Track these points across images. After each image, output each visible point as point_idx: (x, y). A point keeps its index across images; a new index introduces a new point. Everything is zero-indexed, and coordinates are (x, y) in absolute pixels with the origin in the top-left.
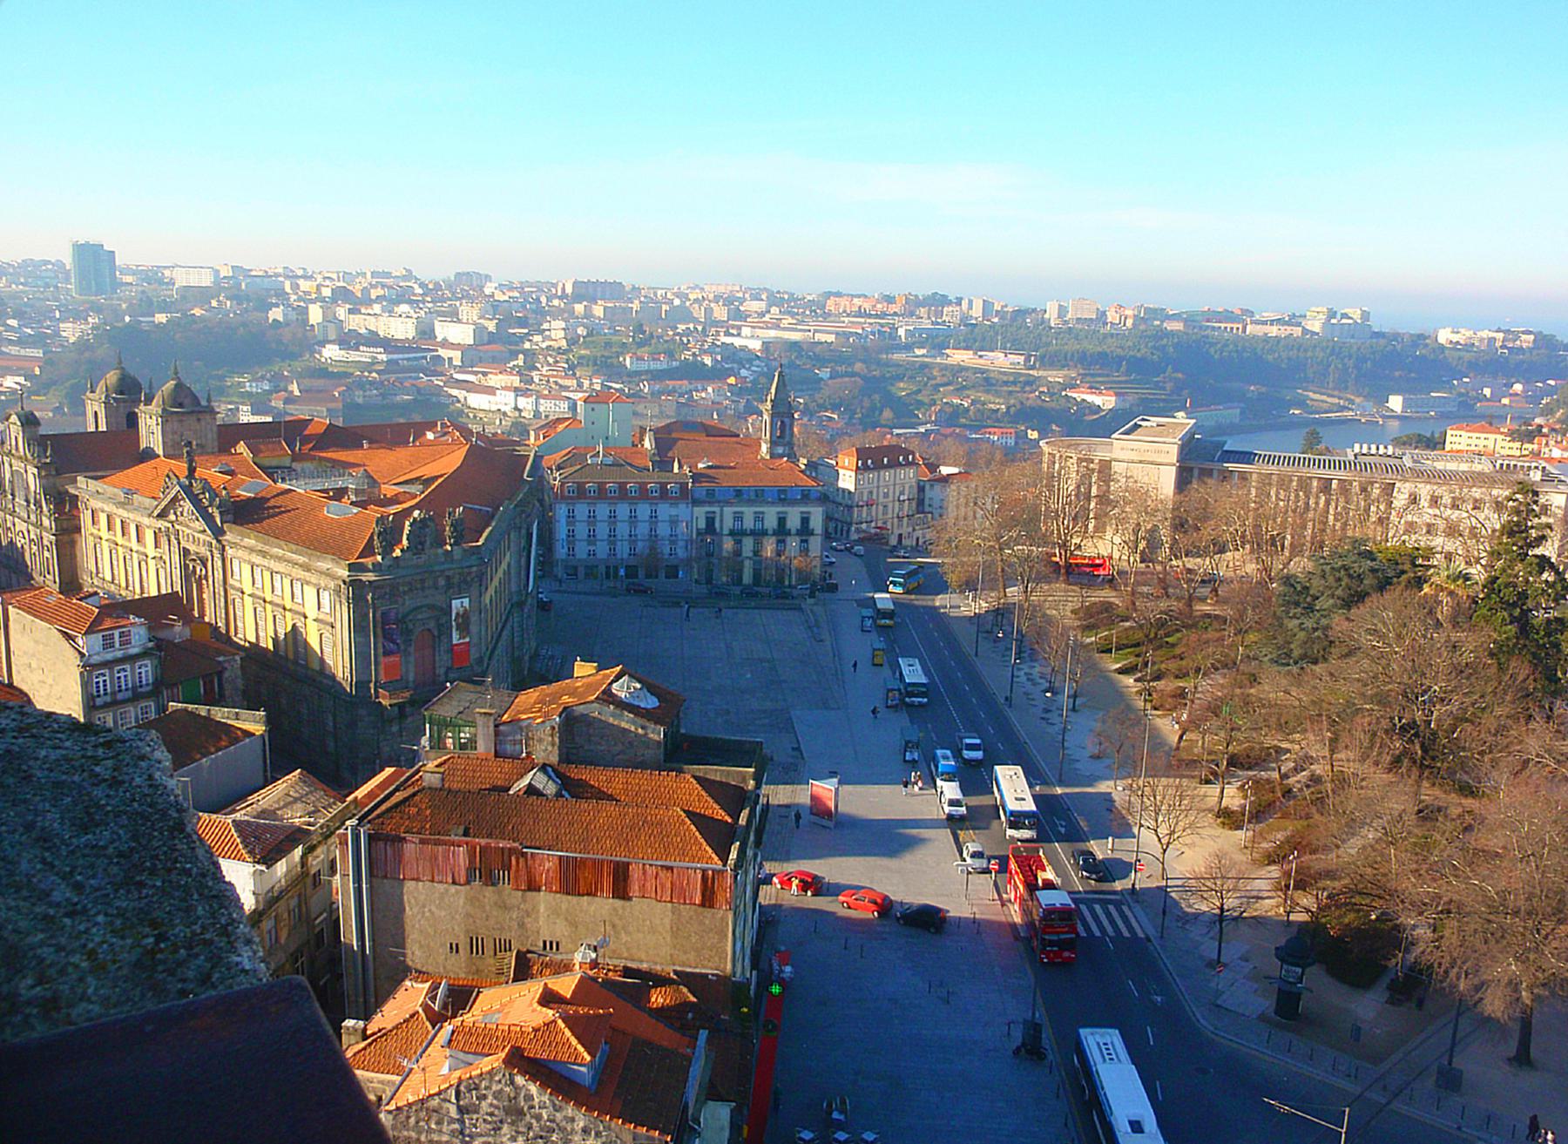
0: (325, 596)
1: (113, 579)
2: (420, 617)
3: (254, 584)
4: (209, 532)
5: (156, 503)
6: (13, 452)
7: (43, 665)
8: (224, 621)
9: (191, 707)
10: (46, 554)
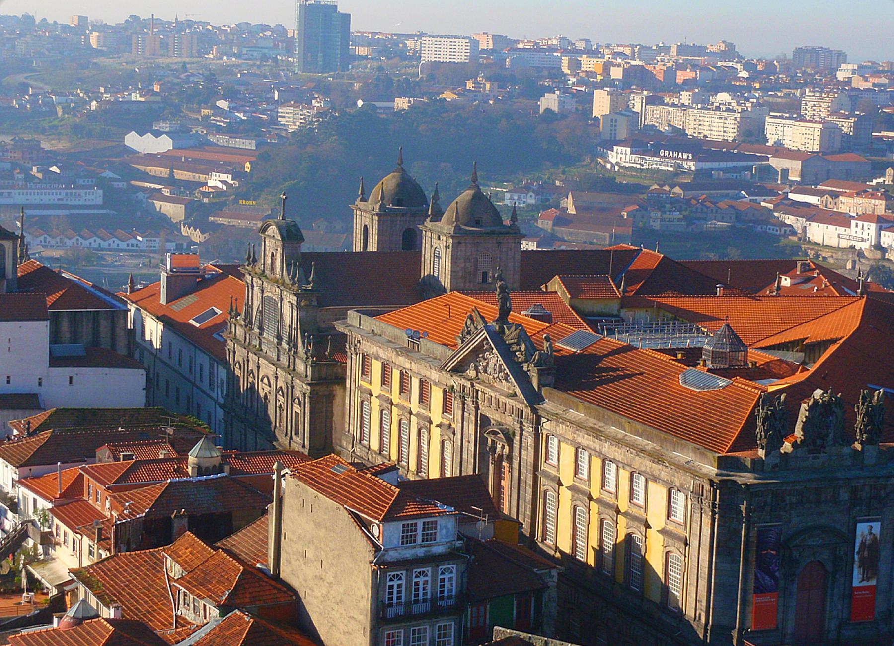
0: (680, 500)
1: (381, 450)
2: (810, 542)
3: (576, 472)
4: (522, 396)
5: (450, 353)
6: (267, 272)
8: (528, 520)
9: (523, 635)
10: (297, 409)
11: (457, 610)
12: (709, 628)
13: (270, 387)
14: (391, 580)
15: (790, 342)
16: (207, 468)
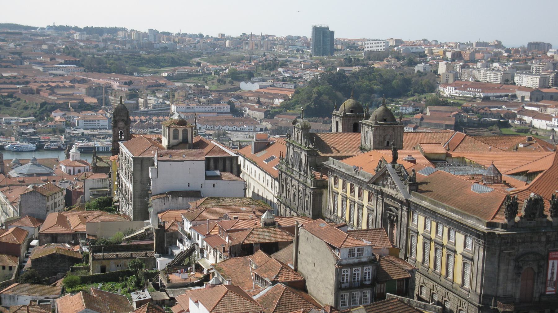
6: (295, 141)
7: (315, 261)
10: (307, 199)
11: (372, 286)
12: (482, 295)
13: (296, 189)
14: (344, 272)
15: (521, 172)
16: (269, 223)
